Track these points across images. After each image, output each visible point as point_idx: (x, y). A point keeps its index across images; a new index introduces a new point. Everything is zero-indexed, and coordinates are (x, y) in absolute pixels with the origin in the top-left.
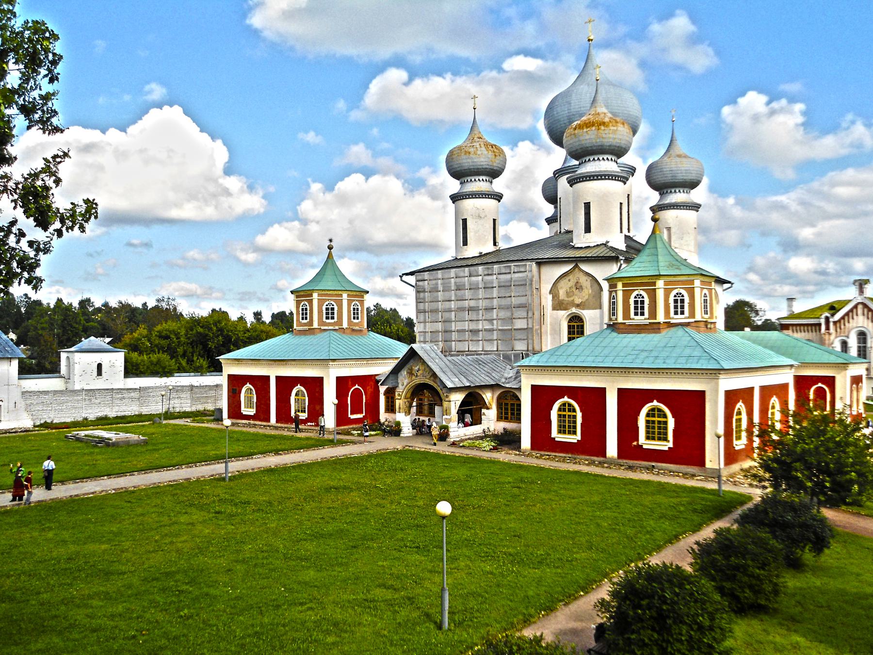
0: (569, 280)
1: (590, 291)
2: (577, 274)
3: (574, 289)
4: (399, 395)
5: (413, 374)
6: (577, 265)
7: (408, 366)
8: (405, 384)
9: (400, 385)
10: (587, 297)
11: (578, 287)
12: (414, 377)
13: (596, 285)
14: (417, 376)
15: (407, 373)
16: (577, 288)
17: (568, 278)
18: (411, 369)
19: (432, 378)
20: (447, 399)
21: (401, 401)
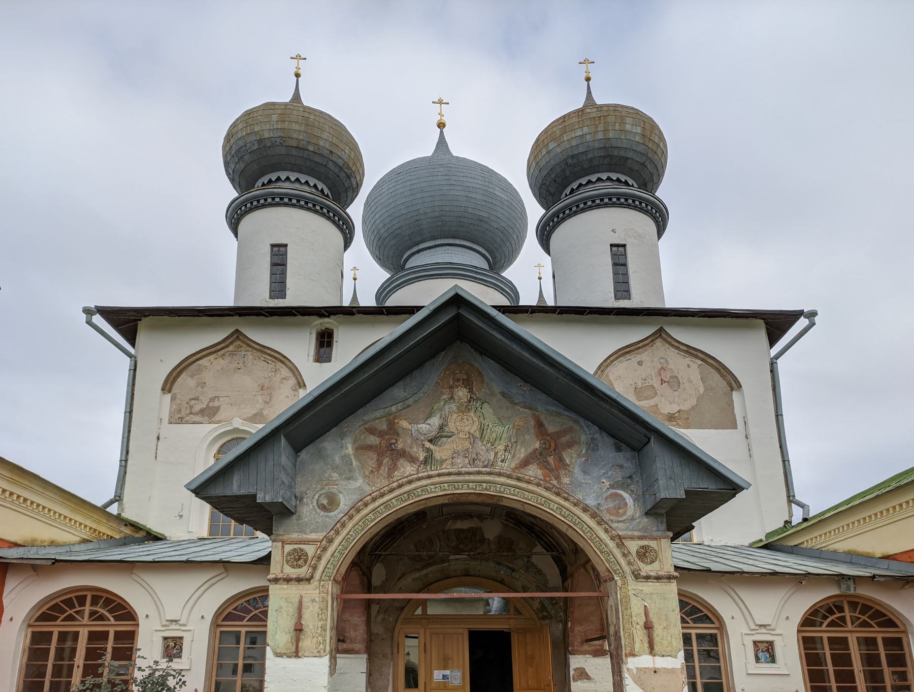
0: (640, 363)
1: (702, 391)
2: (660, 348)
3: (656, 383)
4: (298, 558)
5: (403, 454)
6: (661, 330)
7: (375, 415)
8: (345, 502)
9: (308, 511)
10: (694, 403)
11: (674, 382)
12: (407, 469)
13: (716, 378)
14: (429, 459)
15: (362, 449)
16: (663, 382)
17: (634, 358)
18: (393, 430)
19: (534, 471)
20: (646, 569)
21: (310, 592)
